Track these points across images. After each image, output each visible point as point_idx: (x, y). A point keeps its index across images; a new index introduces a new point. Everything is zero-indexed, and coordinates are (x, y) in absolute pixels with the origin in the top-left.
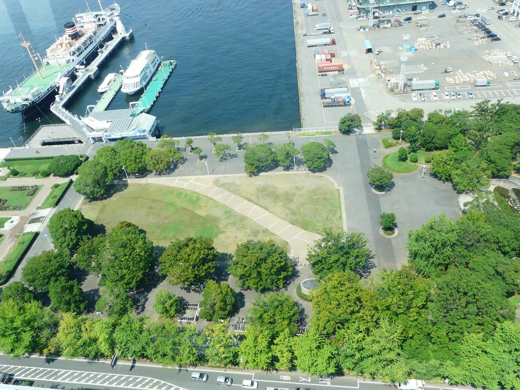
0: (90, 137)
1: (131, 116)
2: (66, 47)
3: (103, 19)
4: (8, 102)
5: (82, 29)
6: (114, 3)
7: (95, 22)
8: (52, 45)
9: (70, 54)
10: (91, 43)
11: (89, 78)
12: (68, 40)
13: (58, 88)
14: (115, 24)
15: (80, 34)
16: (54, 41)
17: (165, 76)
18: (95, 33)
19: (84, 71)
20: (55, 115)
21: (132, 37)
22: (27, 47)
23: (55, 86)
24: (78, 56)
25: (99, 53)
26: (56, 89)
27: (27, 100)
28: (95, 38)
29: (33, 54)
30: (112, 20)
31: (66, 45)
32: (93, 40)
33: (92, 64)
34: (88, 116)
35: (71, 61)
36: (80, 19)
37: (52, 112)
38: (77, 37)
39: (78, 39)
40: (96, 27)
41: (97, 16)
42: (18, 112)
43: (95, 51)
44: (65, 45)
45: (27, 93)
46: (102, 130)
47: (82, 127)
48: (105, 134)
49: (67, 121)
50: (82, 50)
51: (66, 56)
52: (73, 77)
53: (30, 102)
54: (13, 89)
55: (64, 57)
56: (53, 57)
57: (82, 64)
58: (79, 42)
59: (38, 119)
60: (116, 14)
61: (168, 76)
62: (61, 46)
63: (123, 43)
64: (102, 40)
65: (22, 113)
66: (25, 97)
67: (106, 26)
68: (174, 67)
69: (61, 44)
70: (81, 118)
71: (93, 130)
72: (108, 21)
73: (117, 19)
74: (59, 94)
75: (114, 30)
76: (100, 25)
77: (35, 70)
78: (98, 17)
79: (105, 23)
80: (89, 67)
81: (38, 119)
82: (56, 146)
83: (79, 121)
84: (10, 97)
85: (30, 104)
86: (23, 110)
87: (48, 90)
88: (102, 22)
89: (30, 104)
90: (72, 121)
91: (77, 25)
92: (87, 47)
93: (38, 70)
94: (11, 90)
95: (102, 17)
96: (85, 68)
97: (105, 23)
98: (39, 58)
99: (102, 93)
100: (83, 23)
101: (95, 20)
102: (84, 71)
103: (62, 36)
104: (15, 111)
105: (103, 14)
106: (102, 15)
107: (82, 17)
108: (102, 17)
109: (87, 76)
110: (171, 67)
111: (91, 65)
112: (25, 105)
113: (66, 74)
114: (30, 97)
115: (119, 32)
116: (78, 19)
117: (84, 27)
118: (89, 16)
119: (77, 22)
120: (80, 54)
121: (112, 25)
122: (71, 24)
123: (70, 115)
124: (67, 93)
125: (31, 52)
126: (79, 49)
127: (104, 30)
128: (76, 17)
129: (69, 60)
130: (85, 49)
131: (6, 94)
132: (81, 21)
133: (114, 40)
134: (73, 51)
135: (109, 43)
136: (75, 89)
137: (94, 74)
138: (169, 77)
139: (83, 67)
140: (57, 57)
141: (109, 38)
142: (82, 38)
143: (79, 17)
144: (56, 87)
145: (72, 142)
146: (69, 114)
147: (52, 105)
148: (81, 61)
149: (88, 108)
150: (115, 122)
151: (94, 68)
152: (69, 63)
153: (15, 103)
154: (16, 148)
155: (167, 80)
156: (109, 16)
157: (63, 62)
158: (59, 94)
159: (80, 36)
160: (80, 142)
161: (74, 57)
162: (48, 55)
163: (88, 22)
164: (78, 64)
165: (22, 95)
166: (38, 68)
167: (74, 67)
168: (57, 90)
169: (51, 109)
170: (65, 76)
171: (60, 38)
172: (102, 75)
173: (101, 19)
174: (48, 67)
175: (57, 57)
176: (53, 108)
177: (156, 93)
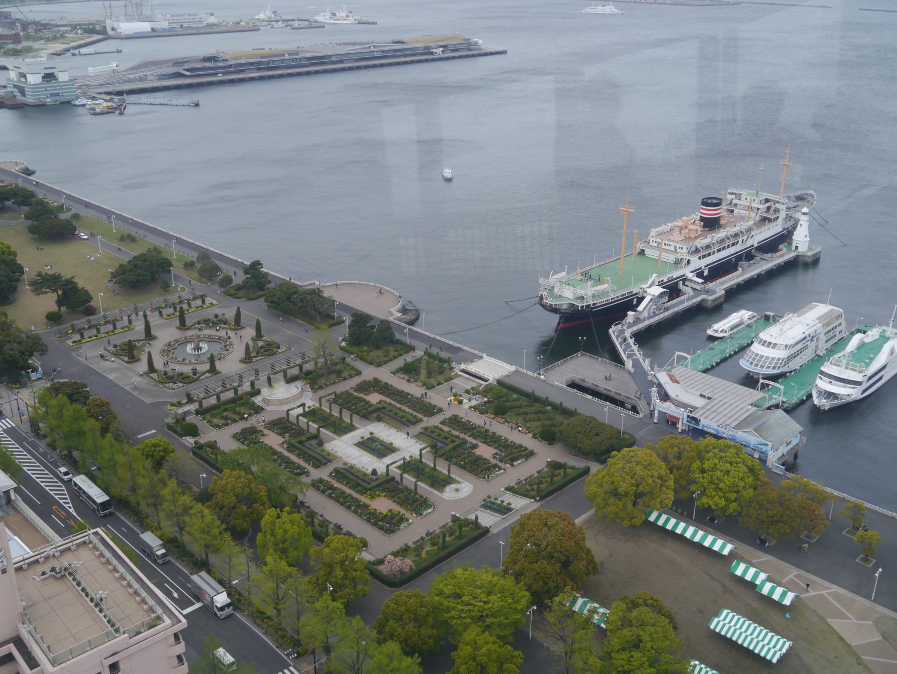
3: (777, 211)
10: (733, 244)
13: (640, 300)
14: (795, 227)
23: (637, 294)
24: (699, 258)
25: (740, 270)
26: (635, 300)
28: (745, 238)
32: (740, 240)
35: (685, 262)
36: (734, 197)
37: (608, 337)
41: (767, 201)
42: (556, 313)
43: (734, 259)
49: (629, 364)
50: (712, 251)
52: (673, 290)
53: (585, 304)
54: (568, 273)
55: (675, 252)
56: (656, 245)
57: (700, 275)
59: (582, 338)
60: (805, 210)
62: (680, 232)
64: (756, 245)
65: (561, 318)
67: (775, 224)
70: (656, 368)
71: (665, 397)
75: (785, 237)
78: (768, 205)
80: (710, 285)
81: (582, 338)
82: (589, 397)
89: (582, 307)
90: (636, 364)
94: (564, 273)
95: (778, 206)
96: (702, 283)
99: (712, 339)
100: (736, 205)
105: (780, 200)
106: (778, 202)
107: (741, 194)
108: (778, 206)
109: (699, 299)
120: (704, 257)
121: (789, 224)
122: (715, 201)
129: (682, 259)
130: (719, 251)
133: (778, 254)
136: (667, 314)
137: (712, 301)
139: (700, 281)
140: (664, 247)
141: (770, 246)
143: (732, 194)
144: (637, 297)
146: (637, 353)
147: (615, 325)
148: (701, 268)
149: (676, 355)
151: (717, 290)
156: (790, 208)
158: (635, 311)
160: (634, 409)
164: (692, 272)
167: (684, 275)
168: (635, 302)
169: (610, 330)
170: (660, 284)
171: (685, 218)
173: (772, 209)
175: (664, 247)
176: (613, 331)
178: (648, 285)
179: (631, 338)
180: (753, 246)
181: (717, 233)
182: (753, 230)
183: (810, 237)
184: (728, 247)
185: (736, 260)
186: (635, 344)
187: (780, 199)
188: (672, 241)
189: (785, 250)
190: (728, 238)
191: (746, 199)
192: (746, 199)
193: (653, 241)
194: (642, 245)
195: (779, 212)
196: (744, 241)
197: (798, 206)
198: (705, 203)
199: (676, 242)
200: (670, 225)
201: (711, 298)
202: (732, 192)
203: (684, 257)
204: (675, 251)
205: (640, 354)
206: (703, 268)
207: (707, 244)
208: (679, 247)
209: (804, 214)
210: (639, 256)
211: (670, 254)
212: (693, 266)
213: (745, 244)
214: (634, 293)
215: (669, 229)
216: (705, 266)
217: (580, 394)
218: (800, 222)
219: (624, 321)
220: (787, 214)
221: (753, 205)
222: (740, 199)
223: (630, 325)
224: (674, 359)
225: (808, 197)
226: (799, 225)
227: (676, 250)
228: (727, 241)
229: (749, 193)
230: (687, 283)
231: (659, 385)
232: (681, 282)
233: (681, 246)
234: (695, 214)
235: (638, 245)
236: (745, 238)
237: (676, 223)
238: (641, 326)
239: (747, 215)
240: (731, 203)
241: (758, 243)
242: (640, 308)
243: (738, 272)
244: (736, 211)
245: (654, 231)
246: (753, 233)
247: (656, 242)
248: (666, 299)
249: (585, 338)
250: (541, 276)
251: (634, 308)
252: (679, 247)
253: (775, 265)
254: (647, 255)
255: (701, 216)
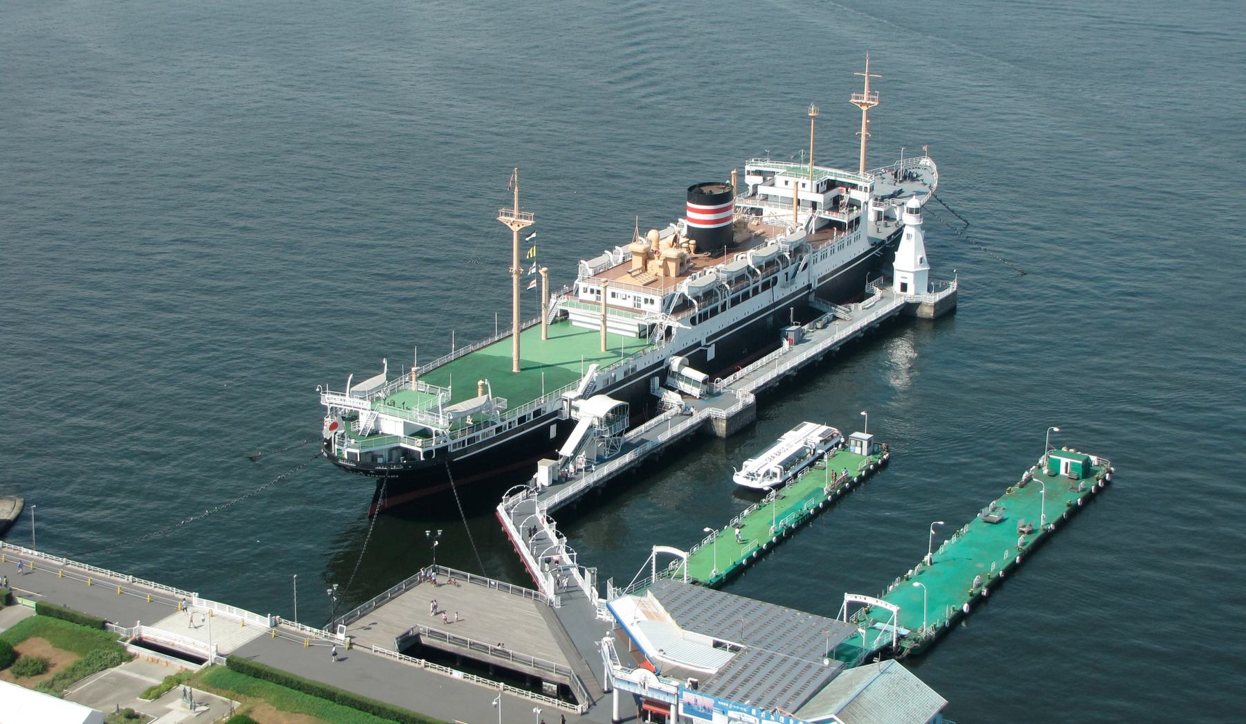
0: (616, 684)
1: (830, 655)
2: (661, 272)
3: (853, 204)
4: (353, 417)
5: (753, 221)
6: (922, 154)
7: (814, 205)
8: (611, 250)
9: (666, 303)
10: (766, 286)
11: (703, 433)
12: (679, 246)
13: (567, 426)
14: (895, 240)
15: (737, 238)
16: (630, 240)
17: (1045, 520)
18: (798, 250)
19: (696, 392)
20: (506, 535)
21: (946, 311)
22: (515, 229)
23: (555, 413)
25: (786, 343)
27: (425, 434)
28: (791, 269)
29: (525, 262)
30: (887, 218)
31: (665, 267)
32: (781, 276)
33: (738, 374)
34: (639, 590)
35: (662, 332)
36: (759, 179)
37: (498, 523)
38: (721, 246)
39: (722, 254)
40: (813, 226)
41: (831, 185)
42: (366, 473)
43: (771, 319)
44: (661, 263)
45: (435, 410)
46: (678, 673)
47: (600, 629)
48: (689, 696)
49: (547, 586)
50: (720, 303)
51: (644, 307)
54: (389, 379)
55: (635, 311)
56: (593, 297)
57: (697, 361)
58: (721, 266)
59: (434, 533)
60: (914, 203)
61: (1056, 518)
62: (645, 264)
63: (904, 319)
64: (815, 285)
66: (424, 421)
68: (1097, 487)
69: (648, 256)
70: (610, 589)
71: (634, 656)
72: (871, 217)
73: (911, 222)
74: (556, 457)
76: (831, 225)
77: (506, 325)
78: (834, 193)
79: (858, 220)
80: (722, 384)
81: (434, 533)
82: (457, 675)
83: (596, 601)
84: (367, 404)
85: (428, 454)
86: (392, 472)
87: (522, 420)
88: (843, 217)
91: (740, 202)
92: (746, 296)
93: (515, 330)
94: (381, 378)
95: (854, 194)
96: (704, 382)
97: (858, 220)
98: (539, 282)
100: (766, 198)
101: (820, 198)
102: (696, 392)
103: (661, 223)
104: (365, 467)
105: (860, 184)
106: (854, 186)
107: (774, 173)
108: (854, 194)
109: (697, 418)
110: (1082, 484)
111: (731, 378)
112: (406, 452)
113: (620, 377)
114: (440, 424)
115: (898, 279)
116: (751, 180)
117: (765, 213)
118: (801, 181)
119: (743, 187)
120: (703, 317)
121: (885, 233)
122: (717, 191)
123: (569, 562)
124: (589, 462)
125: (524, 246)
126: (709, 294)
127: (841, 247)
128: (747, 168)
129: (653, 326)
130: (735, 302)
131: (355, 388)
132: (762, 190)
133: (867, 302)
134: (683, 295)
135: (840, 311)
137: (731, 420)
138: (1062, 524)
139: (700, 376)
142: (741, 255)
145: (534, 684)
147: (511, 494)
148: (698, 344)
149: (653, 555)
150: (748, 657)
151: (739, 395)
152: (647, 341)
153: (374, 433)
154: (294, 627)
155: (1045, 540)
156: (883, 198)
157: (625, 329)
158: (556, 457)
159: (734, 247)
160: (565, 693)
161: (674, 323)
162: (580, 284)
163: (787, 201)
164: (679, 354)
165: (416, 411)
166: (521, 321)
167: (661, 363)
169: (501, 509)
170: (609, 389)
171: (652, 234)
172: (761, 428)
174: (559, 330)
175: (610, 301)
177: (976, 580)
178: (580, 391)
179: (549, 522)
180: (809, 286)
181: (728, 263)
182: (807, 252)
183: (929, 263)
184: (756, 291)
185: (775, 319)
186: (559, 537)
187: (859, 179)
188: (628, 287)
189: (878, 293)
190: (753, 273)
191: (786, 183)
192: (786, 183)
193: (585, 291)
194: (561, 301)
195: (859, 207)
196: (790, 275)
197: (901, 192)
198: (697, 193)
199: (637, 289)
200: (620, 251)
201: (723, 414)
202: (754, 169)
203: (657, 322)
204: (635, 311)
205: (572, 558)
206: (703, 343)
207: (707, 289)
208: (646, 301)
209: (911, 211)
210: (553, 326)
211: (627, 316)
212: (677, 343)
213: (792, 284)
214: (549, 411)
215: (620, 261)
216: (708, 340)
217: (435, 669)
218: (906, 230)
219: (531, 482)
220: (879, 213)
221: (803, 195)
222: (773, 185)
223: (542, 492)
224: (650, 565)
225: (919, 172)
226: (904, 236)
227: (639, 306)
228: (751, 281)
229: (789, 169)
230: (669, 380)
231: (621, 632)
232: (657, 379)
233: (649, 297)
234: (676, 222)
235: (553, 301)
236: (791, 269)
237: (633, 247)
238: (570, 490)
239: (792, 218)
240: (754, 194)
241: (820, 280)
242: (567, 450)
243: (780, 350)
244: (767, 210)
245: (586, 267)
246: (806, 258)
247: (592, 291)
248: (626, 422)
249: (440, 532)
250: (324, 389)
251: (550, 448)
252: (646, 301)
253: (861, 329)
254: (574, 323)
255: (689, 227)
